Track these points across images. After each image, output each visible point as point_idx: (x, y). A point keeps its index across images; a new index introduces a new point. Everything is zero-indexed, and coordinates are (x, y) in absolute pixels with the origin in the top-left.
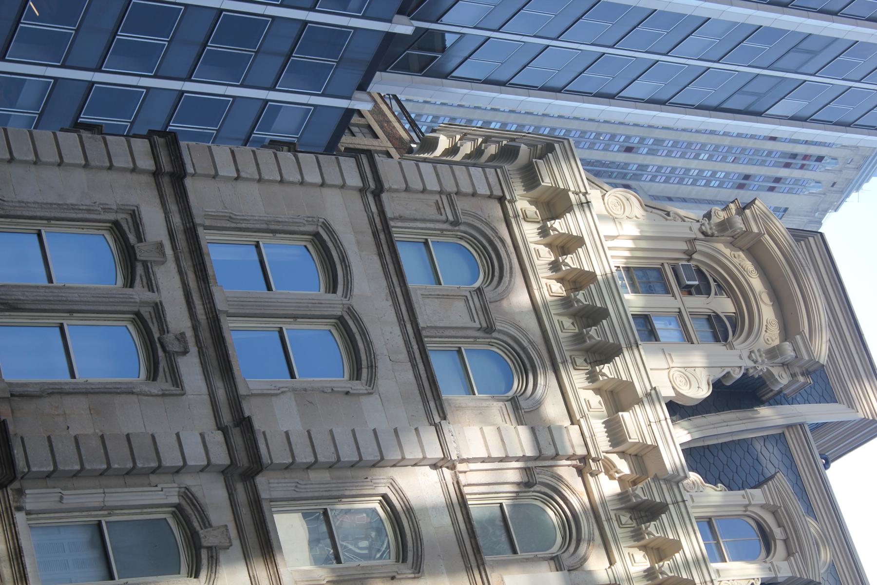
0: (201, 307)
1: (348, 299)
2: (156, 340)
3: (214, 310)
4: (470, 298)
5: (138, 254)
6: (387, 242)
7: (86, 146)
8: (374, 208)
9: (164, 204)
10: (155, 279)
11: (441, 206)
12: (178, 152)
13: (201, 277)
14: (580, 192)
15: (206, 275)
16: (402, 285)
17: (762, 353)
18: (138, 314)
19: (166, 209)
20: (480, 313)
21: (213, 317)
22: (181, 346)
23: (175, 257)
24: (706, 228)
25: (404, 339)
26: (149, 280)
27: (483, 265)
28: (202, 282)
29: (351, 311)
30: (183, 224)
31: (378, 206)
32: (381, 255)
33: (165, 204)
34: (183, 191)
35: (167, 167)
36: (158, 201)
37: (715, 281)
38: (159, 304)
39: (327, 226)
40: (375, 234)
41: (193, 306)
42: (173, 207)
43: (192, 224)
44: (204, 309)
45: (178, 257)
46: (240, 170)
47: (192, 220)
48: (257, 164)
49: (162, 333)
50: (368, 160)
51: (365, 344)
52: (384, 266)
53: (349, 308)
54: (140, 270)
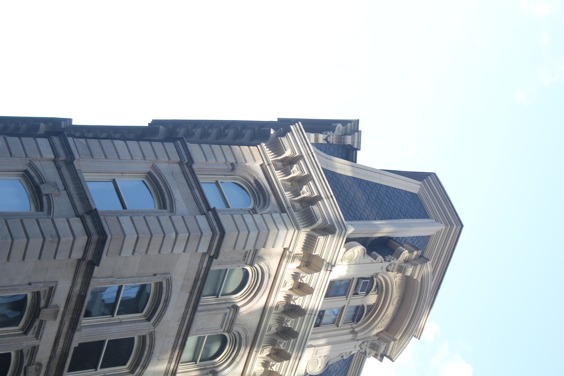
0: (62, 344)
1: (154, 327)
2: (24, 367)
3: (68, 349)
4: (228, 314)
5: (41, 315)
6: (200, 286)
7: (45, 247)
8: (205, 265)
9: (75, 278)
10: (43, 330)
11: (247, 255)
12: (101, 249)
13: (72, 327)
14: (331, 264)
15: (76, 327)
16: (192, 314)
17: (368, 344)
18: (21, 351)
19: (74, 282)
20: (228, 322)
21: (66, 352)
22: (36, 374)
23: (63, 312)
24: (390, 268)
25: (173, 345)
26: (39, 330)
27: (251, 282)
28: (71, 330)
29: (152, 335)
30: (80, 291)
31: (208, 264)
32: (191, 294)
33: (75, 279)
34: (91, 272)
35: (89, 257)
36: (74, 270)
37: (377, 283)
38: (37, 347)
39: (169, 282)
40: (196, 281)
41: (57, 345)
42: (79, 280)
43: (85, 294)
44: (63, 345)
45: (65, 313)
46: (135, 251)
47: (86, 291)
48: (149, 244)
49: (29, 364)
50: (220, 237)
51: (149, 352)
52: (189, 301)
53: (152, 333)
54: (36, 324)
